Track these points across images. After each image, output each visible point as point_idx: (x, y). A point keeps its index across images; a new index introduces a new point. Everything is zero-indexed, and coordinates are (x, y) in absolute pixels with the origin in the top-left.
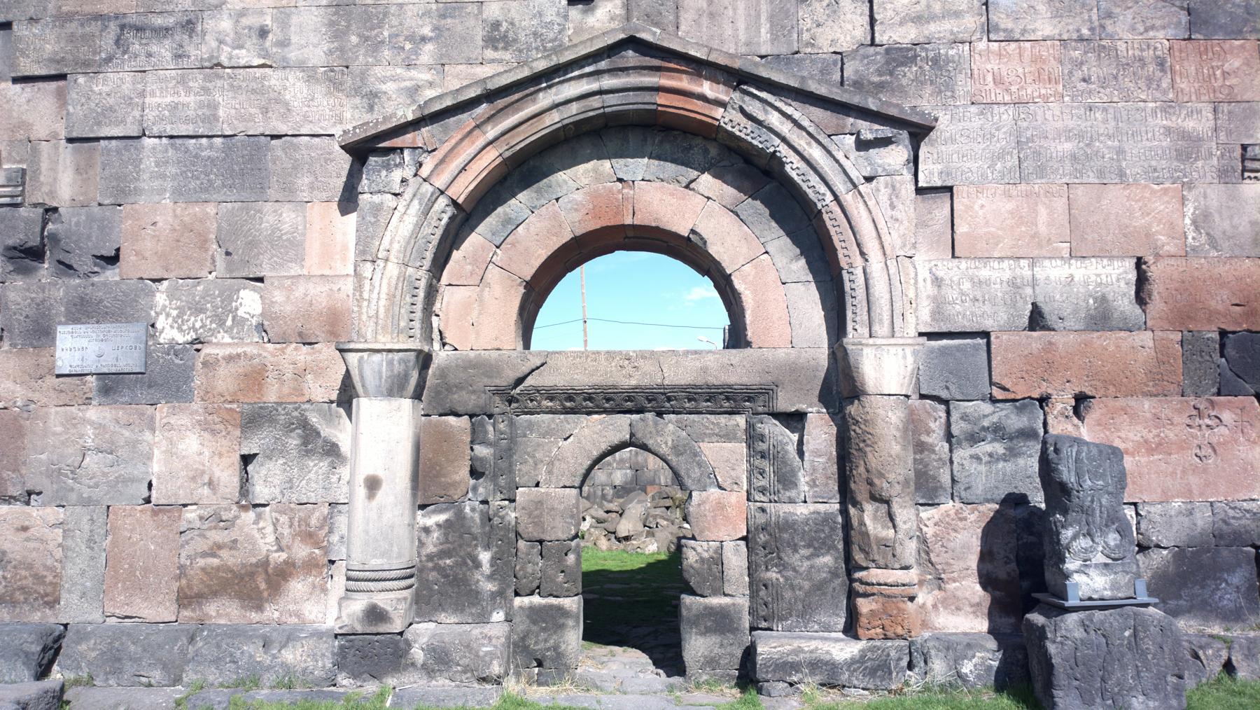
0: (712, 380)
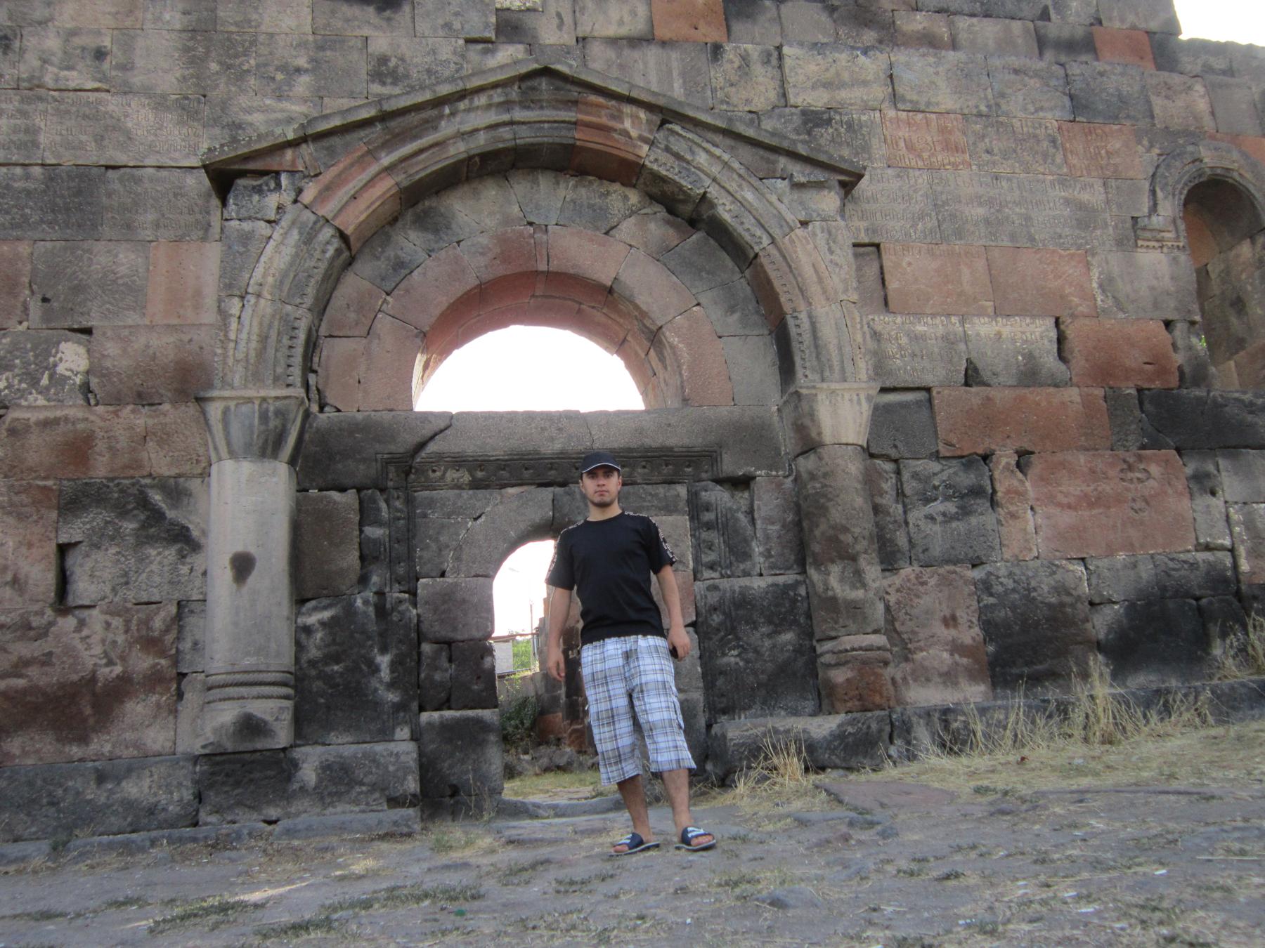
0: (648, 442)
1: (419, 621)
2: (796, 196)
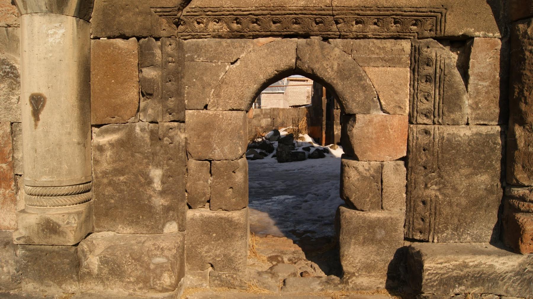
1: (186, 143)
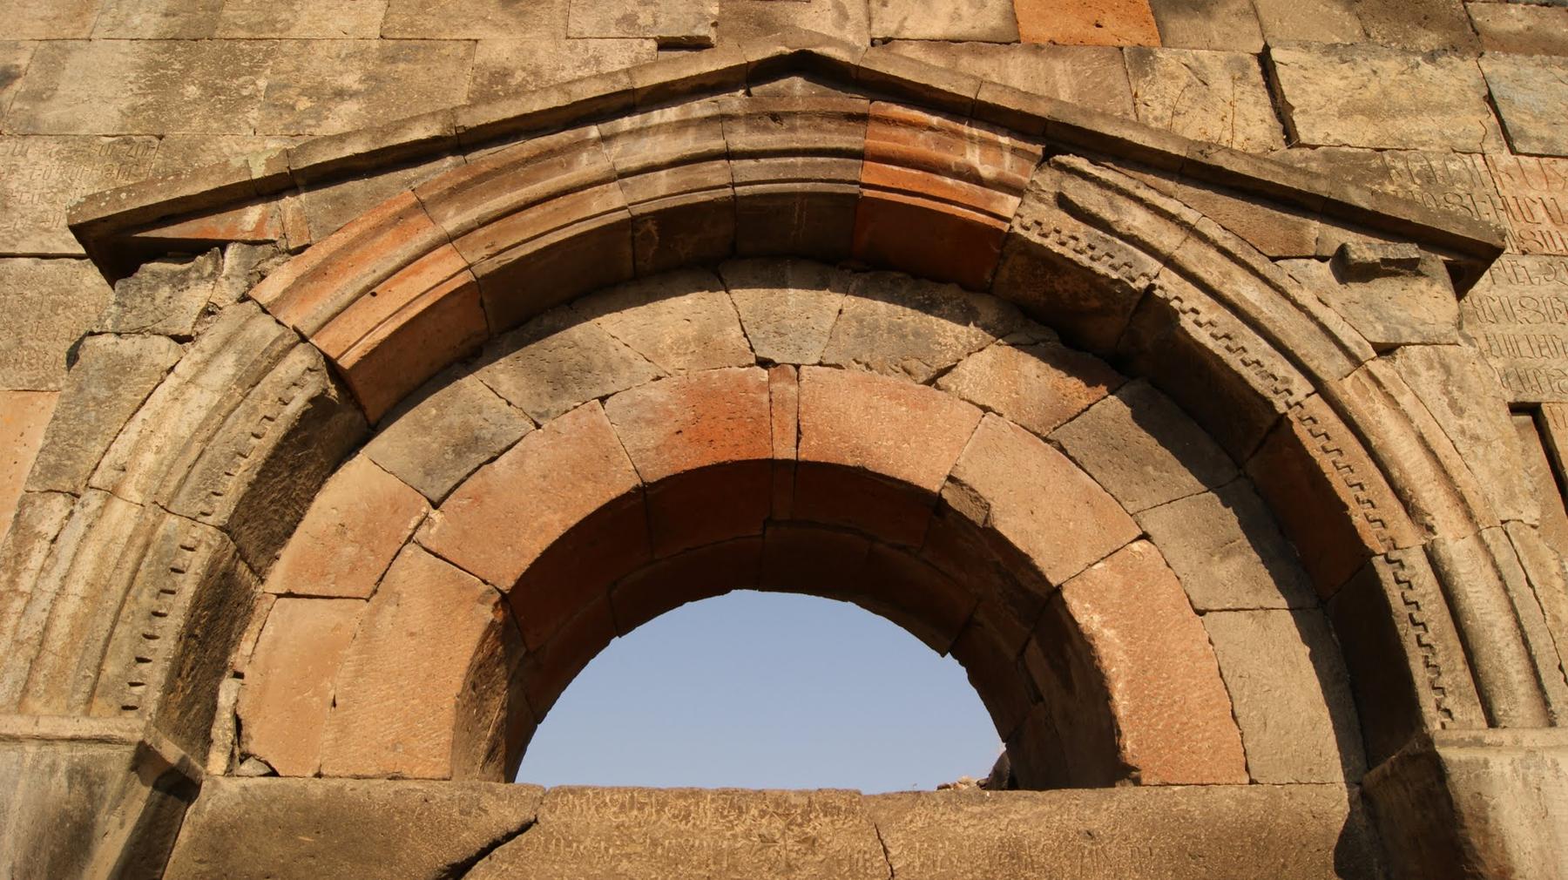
2: (1356, 290)
